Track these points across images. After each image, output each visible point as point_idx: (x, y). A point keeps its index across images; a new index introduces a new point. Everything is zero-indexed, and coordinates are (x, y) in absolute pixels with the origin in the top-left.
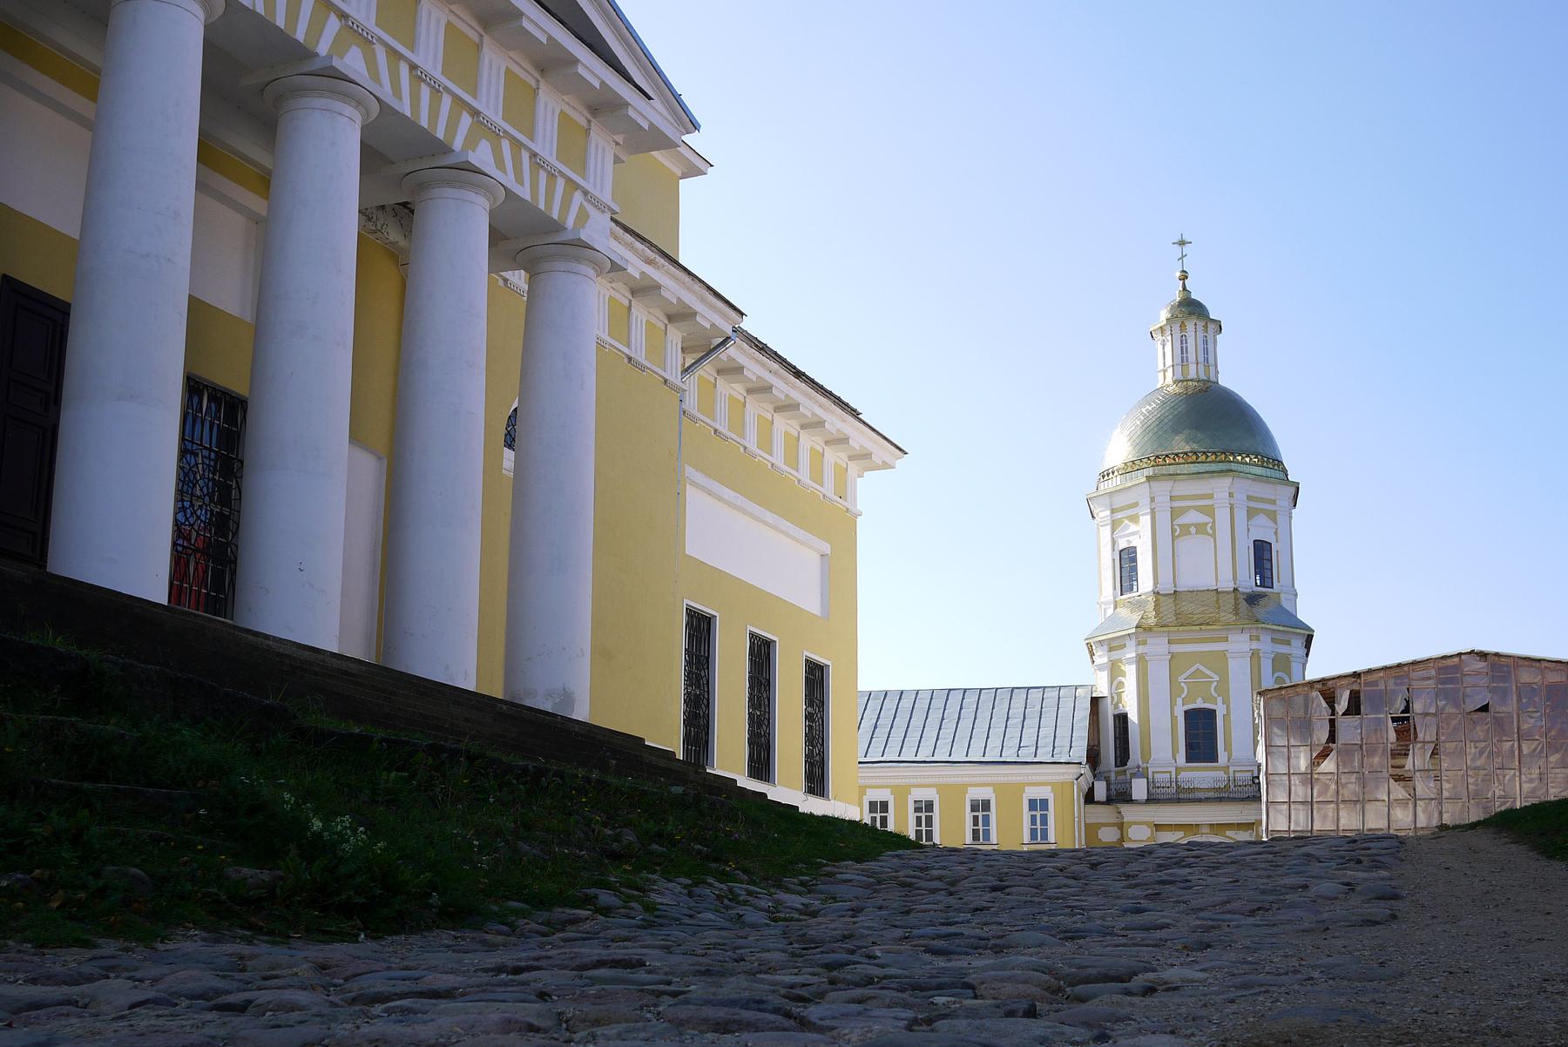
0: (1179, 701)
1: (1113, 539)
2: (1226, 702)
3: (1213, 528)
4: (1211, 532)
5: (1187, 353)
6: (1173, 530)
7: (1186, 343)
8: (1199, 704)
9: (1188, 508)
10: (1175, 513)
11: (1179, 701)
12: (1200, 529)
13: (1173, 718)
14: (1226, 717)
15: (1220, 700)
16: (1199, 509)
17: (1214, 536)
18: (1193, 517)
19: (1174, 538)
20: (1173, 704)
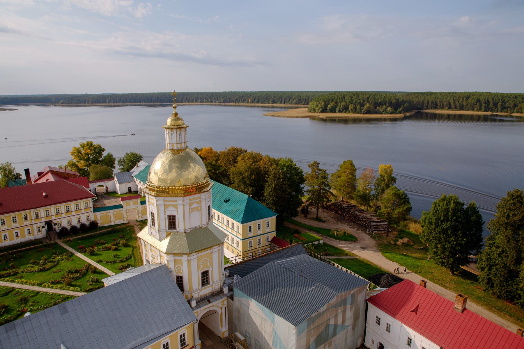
0: (200, 270)
1: (165, 211)
2: (212, 267)
3: (201, 208)
4: (200, 209)
5: (181, 139)
6: (190, 210)
7: (181, 135)
8: (206, 270)
9: (193, 203)
10: (190, 205)
11: (200, 270)
12: (198, 207)
13: (198, 276)
14: (212, 271)
15: (210, 267)
16: (197, 202)
17: (201, 210)
18: (195, 205)
19: (190, 213)
20: (198, 272)
